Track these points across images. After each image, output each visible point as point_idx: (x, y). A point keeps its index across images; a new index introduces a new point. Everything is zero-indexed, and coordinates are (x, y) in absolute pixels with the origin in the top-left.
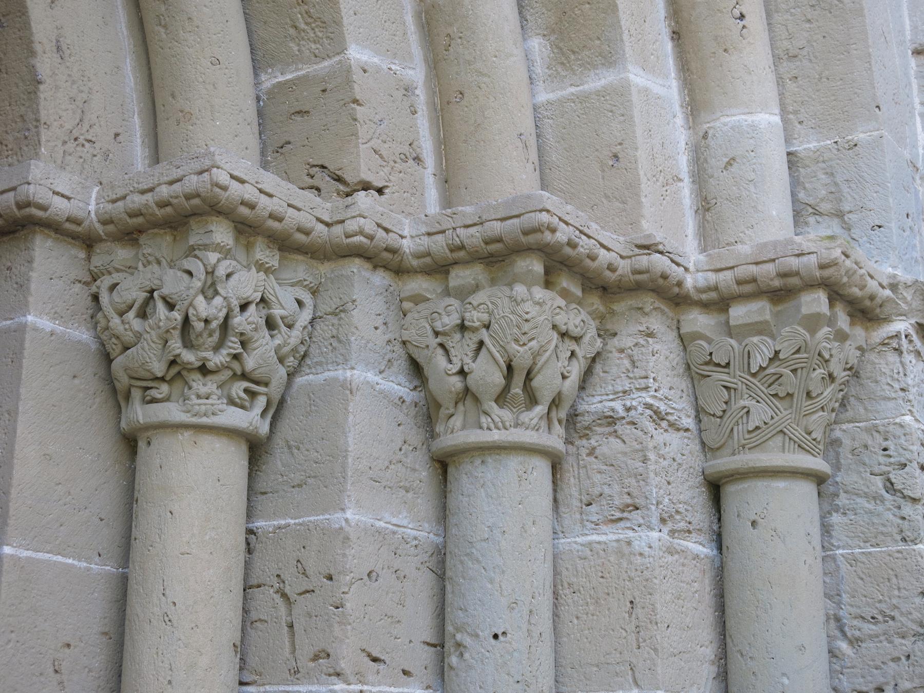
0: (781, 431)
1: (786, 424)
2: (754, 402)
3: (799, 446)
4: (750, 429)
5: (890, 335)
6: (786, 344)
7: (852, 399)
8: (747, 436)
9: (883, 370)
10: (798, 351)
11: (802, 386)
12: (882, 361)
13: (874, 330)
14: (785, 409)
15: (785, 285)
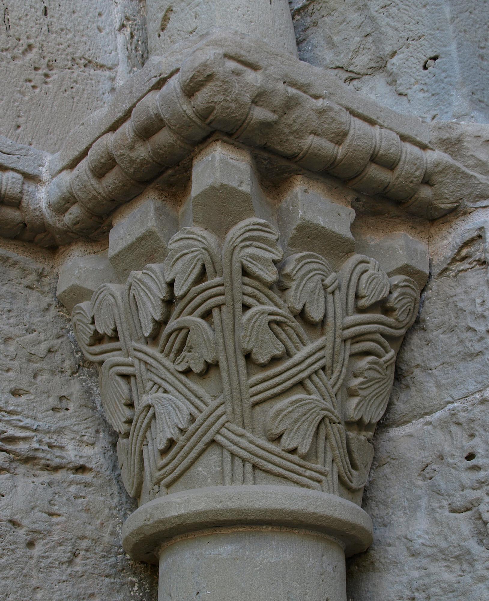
0: (213, 442)
1: (217, 425)
2: (160, 394)
3: (255, 467)
4: (162, 447)
5: (467, 237)
6: (179, 265)
7: (417, 372)
8: (161, 463)
9: (460, 305)
10: (202, 276)
11: (230, 343)
12: (458, 290)
13: (444, 238)
14: (214, 397)
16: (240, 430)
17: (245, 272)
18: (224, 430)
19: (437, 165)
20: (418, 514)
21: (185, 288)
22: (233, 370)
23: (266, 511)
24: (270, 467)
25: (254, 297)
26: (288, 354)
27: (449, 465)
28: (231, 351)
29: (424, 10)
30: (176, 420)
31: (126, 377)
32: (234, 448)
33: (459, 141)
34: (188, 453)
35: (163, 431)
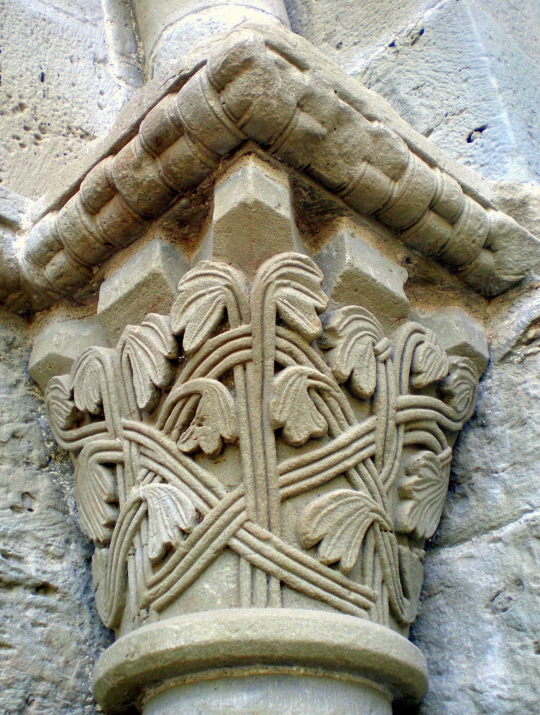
0: (227, 548)
1: (233, 525)
2: (156, 484)
6: (192, 310)
7: (477, 477)
8: (152, 578)
10: (223, 323)
11: (255, 413)
12: (528, 376)
13: (503, 319)
14: (230, 488)
15: (168, 170)
16: (265, 532)
17: (281, 320)
18: (242, 533)
19: (502, 226)
20: (489, 658)
21: (198, 340)
22: (259, 450)
23: (300, 645)
24: (304, 584)
25: (290, 353)
26: (330, 434)
27: (531, 591)
28: (256, 424)
29: (464, 85)
30: (177, 518)
31: (110, 466)
32: (256, 557)
33: (524, 203)
34: (191, 564)
35: (157, 533)
